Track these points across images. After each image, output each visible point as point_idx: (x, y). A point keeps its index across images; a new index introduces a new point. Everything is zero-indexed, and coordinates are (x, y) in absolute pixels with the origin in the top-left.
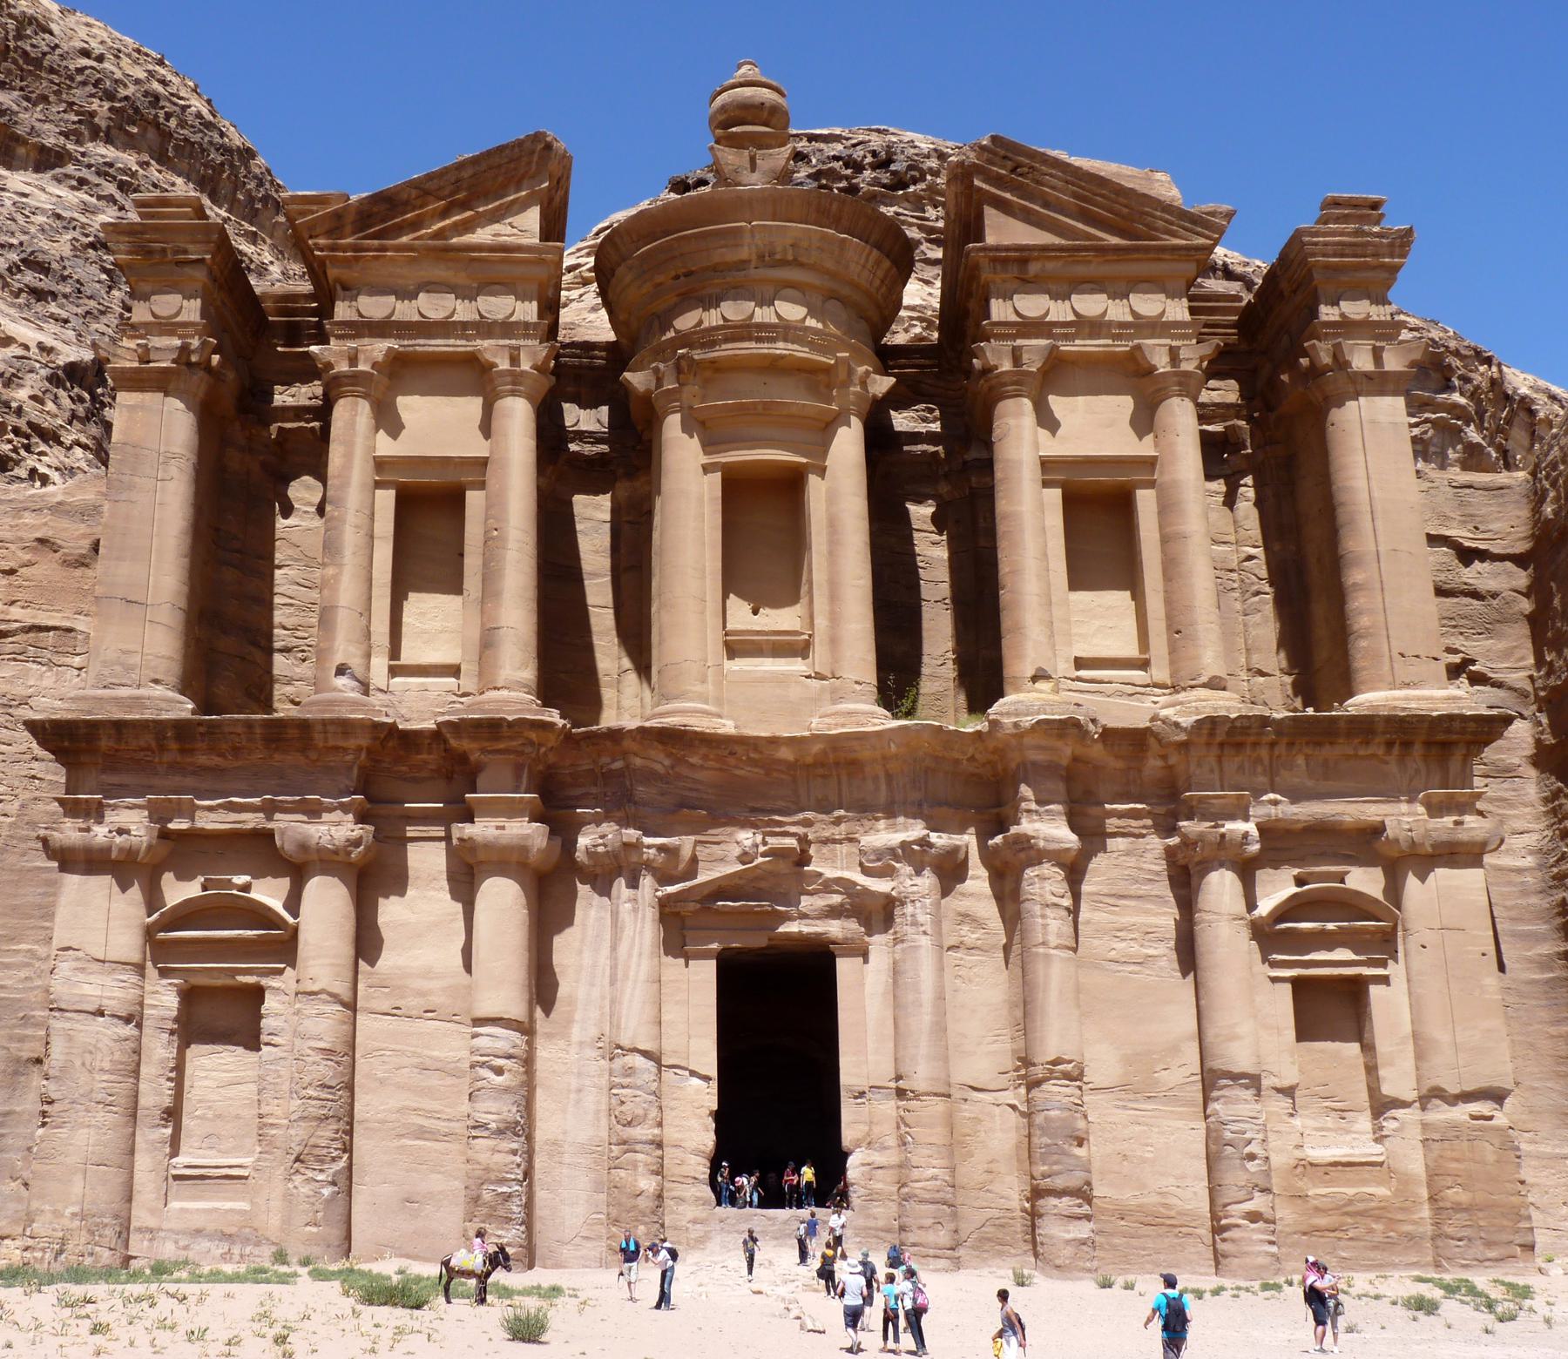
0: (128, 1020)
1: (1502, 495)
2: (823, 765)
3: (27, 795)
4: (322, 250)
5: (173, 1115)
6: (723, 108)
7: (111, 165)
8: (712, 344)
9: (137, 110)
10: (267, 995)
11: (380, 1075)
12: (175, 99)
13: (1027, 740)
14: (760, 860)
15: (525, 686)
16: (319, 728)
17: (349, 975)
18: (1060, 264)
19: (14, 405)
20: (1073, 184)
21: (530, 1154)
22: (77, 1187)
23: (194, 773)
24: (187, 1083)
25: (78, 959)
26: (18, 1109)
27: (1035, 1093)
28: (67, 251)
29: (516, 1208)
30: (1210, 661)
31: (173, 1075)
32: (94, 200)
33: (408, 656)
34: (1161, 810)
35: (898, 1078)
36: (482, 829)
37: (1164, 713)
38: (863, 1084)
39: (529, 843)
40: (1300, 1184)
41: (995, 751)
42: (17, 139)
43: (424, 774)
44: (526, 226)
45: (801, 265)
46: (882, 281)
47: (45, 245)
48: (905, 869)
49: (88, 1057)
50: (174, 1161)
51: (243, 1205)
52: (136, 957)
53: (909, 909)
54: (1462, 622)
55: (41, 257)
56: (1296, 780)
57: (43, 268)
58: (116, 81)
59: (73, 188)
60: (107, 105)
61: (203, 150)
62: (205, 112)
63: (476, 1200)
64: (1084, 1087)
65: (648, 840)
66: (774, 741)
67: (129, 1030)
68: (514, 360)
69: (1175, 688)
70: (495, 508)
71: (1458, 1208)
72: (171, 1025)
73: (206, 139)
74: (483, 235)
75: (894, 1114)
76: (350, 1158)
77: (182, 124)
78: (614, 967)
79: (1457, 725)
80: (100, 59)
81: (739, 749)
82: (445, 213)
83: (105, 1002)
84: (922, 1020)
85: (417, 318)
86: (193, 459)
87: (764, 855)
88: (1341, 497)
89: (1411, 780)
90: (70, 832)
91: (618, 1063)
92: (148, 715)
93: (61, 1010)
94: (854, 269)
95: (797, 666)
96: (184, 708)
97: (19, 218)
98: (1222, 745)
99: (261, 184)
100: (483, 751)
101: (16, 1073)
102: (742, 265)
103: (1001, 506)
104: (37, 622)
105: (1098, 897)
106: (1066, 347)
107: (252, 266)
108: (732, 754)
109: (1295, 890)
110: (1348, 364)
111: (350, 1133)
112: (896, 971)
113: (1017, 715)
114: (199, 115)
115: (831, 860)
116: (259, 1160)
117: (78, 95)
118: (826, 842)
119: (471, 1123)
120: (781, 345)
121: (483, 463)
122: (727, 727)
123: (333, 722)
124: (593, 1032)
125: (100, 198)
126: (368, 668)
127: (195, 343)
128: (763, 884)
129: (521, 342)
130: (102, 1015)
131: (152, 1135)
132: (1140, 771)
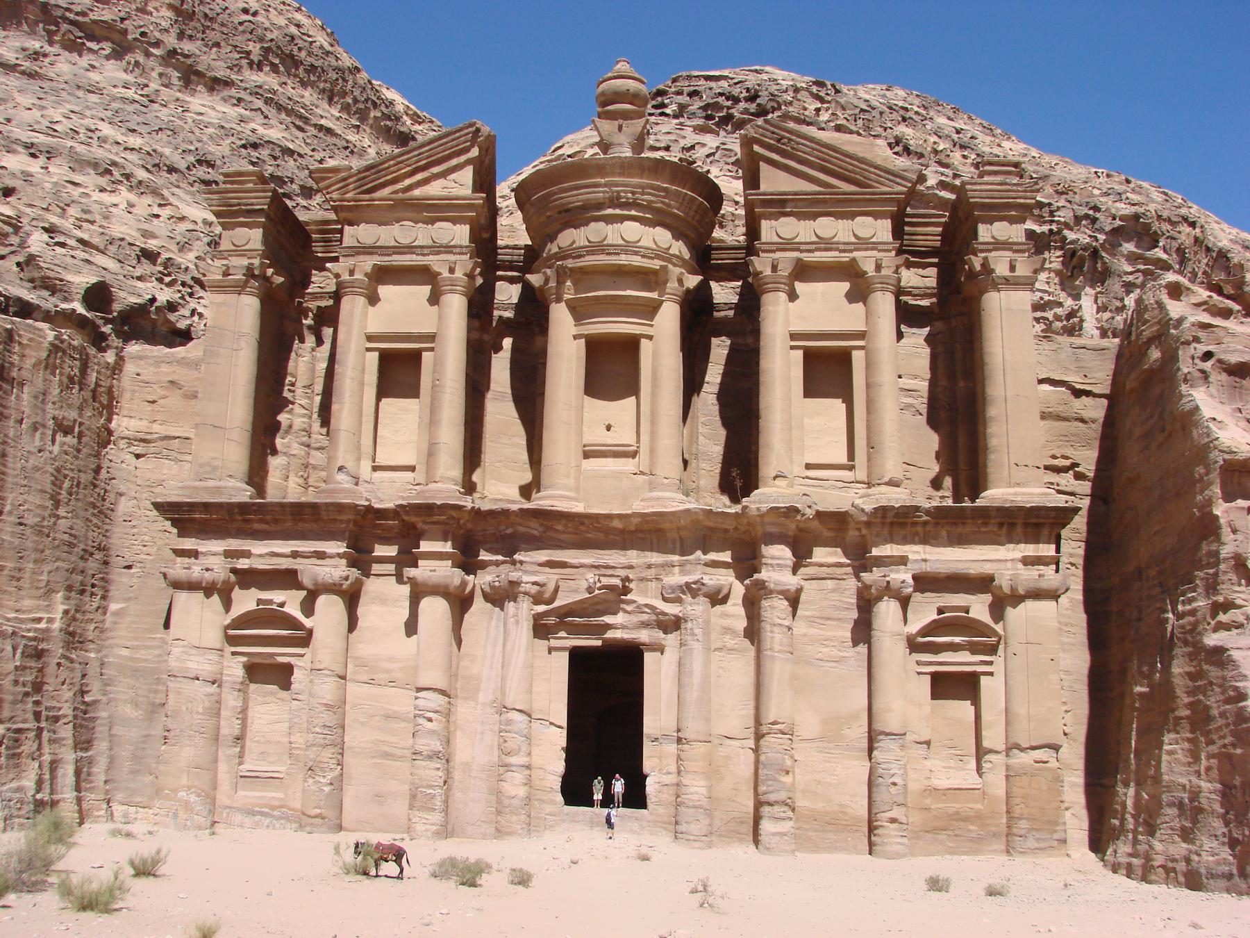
0: (213, 683)
1: (1104, 354)
2: (641, 531)
4: (334, 201)
5: (240, 738)
6: (603, 94)
7: (260, 87)
8: (580, 256)
9: (278, 47)
10: (295, 670)
11: (362, 720)
12: (306, 38)
13: (766, 519)
14: (597, 592)
15: (454, 480)
16: (324, 508)
17: (342, 660)
19: (183, 267)
20: (817, 150)
21: (448, 772)
22: (184, 780)
24: (249, 721)
26: (153, 733)
28: (227, 152)
29: (438, 802)
30: (891, 467)
31: (240, 716)
32: (247, 113)
34: (857, 563)
35: (679, 731)
36: (425, 571)
37: (858, 502)
39: (449, 581)
44: (461, 184)
46: (696, 212)
48: (687, 598)
49: (190, 706)
50: (241, 767)
51: (280, 795)
52: (218, 646)
53: (689, 625)
54: (1072, 438)
55: (209, 158)
57: (211, 165)
58: (266, 29)
59: (235, 105)
60: (258, 46)
61: (323, 71)
63: (413, 797)
64: (794, 738)
65: (526, 578)
66: (609, 517)
68: (452, 271)
69: (869, 485)
70: (438, 366)
72: (238, 687)
73: (326, 63)
74: (435, 189)
79: (1043, 513)
80: (255, 14)
81: (586, 521)
83: (200, 672)
84: (692, 695)
85: (393, 243)
86: (257, 335)
87: (599, 589)
88: (987, 359)
90: (179, 568)
91: (504, 717)
92: (223, 499)
95: (628, 465)
97: (197, 131)
98: (892, 524)
100: (424, 522)
101: (152, 712)
103: (763, 364)
104: (168, 433)
105: (811, 621)
106: (806, 257)
107: (355, 150)
108: (582, 524)
109: (935, 617)
110: (993, 271)
111: (342, 754)
113: (760, 503)
114: (321, 47)
115: (644, 593)
116: (289, 769)
117: (239, 40)
118: (642, 580)
119: (413, 751)
120: (623, 257)
121: (431, 338)
122: (579, 508)
124: (491, 697)
125: (252, 110)
127: (256, 262)
128: (599, 607)
130: (198, 679)
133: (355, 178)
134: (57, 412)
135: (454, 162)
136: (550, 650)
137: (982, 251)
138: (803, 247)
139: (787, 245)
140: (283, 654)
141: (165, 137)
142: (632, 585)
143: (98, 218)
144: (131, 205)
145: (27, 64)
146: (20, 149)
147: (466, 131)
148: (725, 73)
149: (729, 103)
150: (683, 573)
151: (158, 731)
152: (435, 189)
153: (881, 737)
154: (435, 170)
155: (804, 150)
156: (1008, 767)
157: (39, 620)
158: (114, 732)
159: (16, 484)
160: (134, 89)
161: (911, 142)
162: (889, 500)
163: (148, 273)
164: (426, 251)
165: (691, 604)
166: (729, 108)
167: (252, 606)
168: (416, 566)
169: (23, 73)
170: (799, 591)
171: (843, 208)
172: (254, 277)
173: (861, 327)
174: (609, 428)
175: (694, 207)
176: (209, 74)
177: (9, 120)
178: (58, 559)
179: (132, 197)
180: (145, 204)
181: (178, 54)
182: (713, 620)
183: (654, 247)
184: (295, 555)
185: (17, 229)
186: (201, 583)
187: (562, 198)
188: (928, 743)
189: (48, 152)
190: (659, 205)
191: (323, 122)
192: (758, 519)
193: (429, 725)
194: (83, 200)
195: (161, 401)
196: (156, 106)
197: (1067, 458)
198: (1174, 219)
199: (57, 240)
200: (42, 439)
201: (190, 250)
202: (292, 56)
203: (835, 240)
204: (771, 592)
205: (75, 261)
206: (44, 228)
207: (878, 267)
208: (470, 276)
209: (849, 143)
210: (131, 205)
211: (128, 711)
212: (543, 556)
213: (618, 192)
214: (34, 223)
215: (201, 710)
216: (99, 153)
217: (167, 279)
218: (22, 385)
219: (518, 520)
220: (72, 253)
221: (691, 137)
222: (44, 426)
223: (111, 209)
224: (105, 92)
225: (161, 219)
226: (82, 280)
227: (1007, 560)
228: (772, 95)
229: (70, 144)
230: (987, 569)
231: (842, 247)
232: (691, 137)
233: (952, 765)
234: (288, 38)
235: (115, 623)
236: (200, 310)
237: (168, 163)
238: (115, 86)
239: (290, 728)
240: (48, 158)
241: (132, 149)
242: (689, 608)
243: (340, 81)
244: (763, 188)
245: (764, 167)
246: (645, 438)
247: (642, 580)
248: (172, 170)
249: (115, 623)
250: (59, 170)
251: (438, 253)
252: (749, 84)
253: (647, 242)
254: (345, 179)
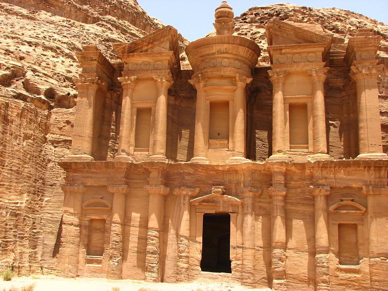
7: (109, 20)
9: (116, 6)
18: (290, 50)
23: (92, 173)
28: (98, 43)
32: (105, 29)
40: (337, 273)
42: (88, 16)
43: (141, 173)
45: (227, 53)
46: (250, 55)
56: (341, 176)
59: (100, 27)
60: (109, 6)
66: (217, 166)
69: (314, 153)
71: (376, 281)
77: (127, 8)
81: (210, 168)
82: (148, 45)
89: (370, 176)
94: (241, 53)
97: (87, 36)
98: (322, 167)
99: (146, 20)
102: (214, 54)
122: (207, 163)
123: (119, 162)
125: (107, 28)
126: (129, 149)
128: (214, 199)
132: (304, 173)
145: (31, 15)
146: (26, 43)
157: (17, 203)
159: (10, 156)
161: (339, 28)
162: (321, 159)
178: (25, 182)
179: (63, 59)
191: (132, 32)
195: (63, 128)
196: (73, 28)
199: (36, 74)
200: (19, 141)
205: (42, 81)
209: (306, 26)
214: (28, 68)
216: (52, 44)
218: (12, 122)
219: (184, 168)
220: (41, 78)
221: (255, 30)
226: (44, 87)
228: (285, 13)
232: (255, 30)
238: (60, 21)
241: (65, 43)
250: (39, 50)
252: (277, 10)
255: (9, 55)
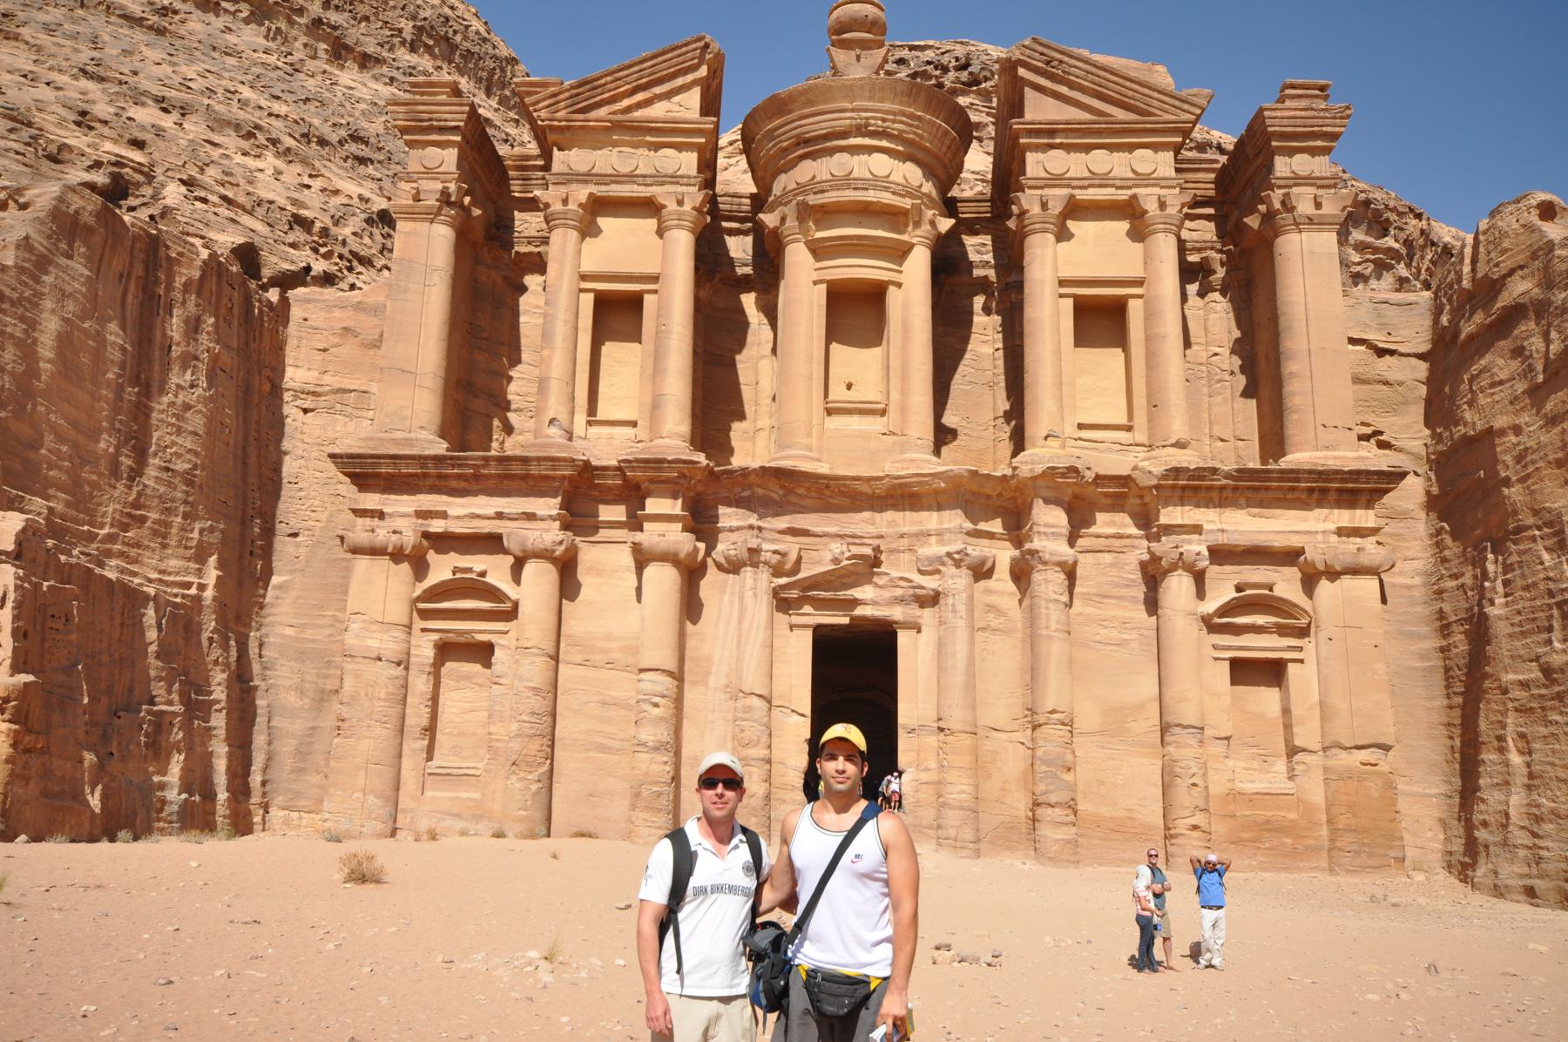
0: (399, 664)
3: (334, 508)
5: (431, 730)
6: (838, 21)
7: (414, 68)
10: (496, 649)
13: (1040, 483)
14: (846, 562)
17: (553, 637)
19: (340, 238)
22: (361, 780)
25: (364, 621)
26: (322, 725)
27: (1037, 733)
28: (381, 130)
30: (1178, 427)
32: (401, 93)
33: (602, 414)
35: (940, 719)
36: (652, 535)
37: (1141, 464)
38: (913, 724)
41: (1017, 489)
44: (689, 105)
46: (949, 148)
47: (365, 125)
49: (370, 690)
53: (950, 601)
54: (1374, 403)
55: (362, 134)
58: (418, 7)
59: (386, 84)
60: (411, 24)
61: (480, 58)
62: (482, 30)
63: (637, 795)
67: (399, 671)
68: (680, 203)
70: (661, 308)
72: (428, 669)
74: (658, 110)
75: (936, 744)
76: (552, 764)
77: (465, 38)
78: (740, 635)
83: (382, 652)
85: (610, 171)
86: (451, 271)
87: (848, 559)
88: (1282, 308)
90: (360, 532)
91: (740, 703)
92: (415, 452)
93: (351, 656)
95: (875, 424)
96: (441, 448)
97: (348, 105)
101: (321, 700)
104: (343, 386)
105: (1087, 598)
111: (552, 746)
112: (940, 645)
113: (1033, 463)
114: (477, 33)
118: (892, 551)
119: (636, 742)
120: (871, 192)
121: (655, 279)
122: (823, 469)
124: (724, 681)
126: (572, 422)
127: (452, 187)
129: (685, 189)
130: (380, 660)
131: (414, 745)
133: (567, 94)
134: (212, 345)
135: (680, 81)
136: (792, 627)
137: (1279, 187)
138: (1075, 183)
139: (1056, 180)
140: (481, 630)
141: (313, 109)
142: (883, 557)
143: (242, 182)
144: (278, 172)
145: (155, 18)
146: (150, 102)
147: (694, 46)
148: (931, 43)
149: (938, 73)
150: (941, 542)
151: (329, 722)
152: (658, 110)
153: (1177, 730)
154: (658, 90)
155: (1077, 72)
156: (1326, 769)
157: (188, 585)
158: (273, 723)
159: (162, 421)
160: (276, 56)
163: (302, 239)
164: (648, 181)
165: (952, 577)
166: (936, 77)
167: (448, 575)
168: (641, 530)
169: (150, 28)
170: (1075, 563)
171: (1119, 138)
172: (449, 204)
173: (1136, 272)
174: (849, 387)
175: (947, 142)
176: (358, 49)
177: (135, 73)
179: (280, 164)
180: (293, 173)
181: (323, 24)
182: (976, 596)
183: (904, 182)
184: (500, 516)
185: (150, 178)
186: (386, 548)
187: (801, 126)
188: (1228, 738)
189: (182, 108)
190: (911, 136)
192: (1030, 483)
193: (656, 711)
194: (224, 162)
196: (302, 76)
197: (1368, 425)
198: (1400, 209)
201: (345, 225)
202: (446, 39)
203: (1111, 175)
204: (1045, 563)
205: (218, 219)
206: (181, 180)
207: (1162, 205)
208: (698, 210)
210: (278, 172)
211: (292, 699)
212: (783, 522)
213: (867, 118)
215: (383, 695)
217: (323, 250)
219: (758, 481)
222: (196, 358)
223: (256, 174)
224: (244, 55)
225: (313, 190)
227: (1317, 532)
229: (206, 101)
230: (1295, 541)
231: (1118, 183)
233: (1255, 766)
234: (442, 19)
235: (277, 598)
236: (359, 284)
237: (317, 133)
239: (490, 717)
240: (183, 115)
241: (277, 116)
242: (950, 581)
243: (498, 71)
244: (1028, 116)
245: (1029, 93)
246: (895, 396)
247: (892, 551)
248: (322, 142)
249: (277, 598)
250: (195, 128)
251: (662, 184)
253: (896, 177)
254: (554, 95)
255: (91, 128)
